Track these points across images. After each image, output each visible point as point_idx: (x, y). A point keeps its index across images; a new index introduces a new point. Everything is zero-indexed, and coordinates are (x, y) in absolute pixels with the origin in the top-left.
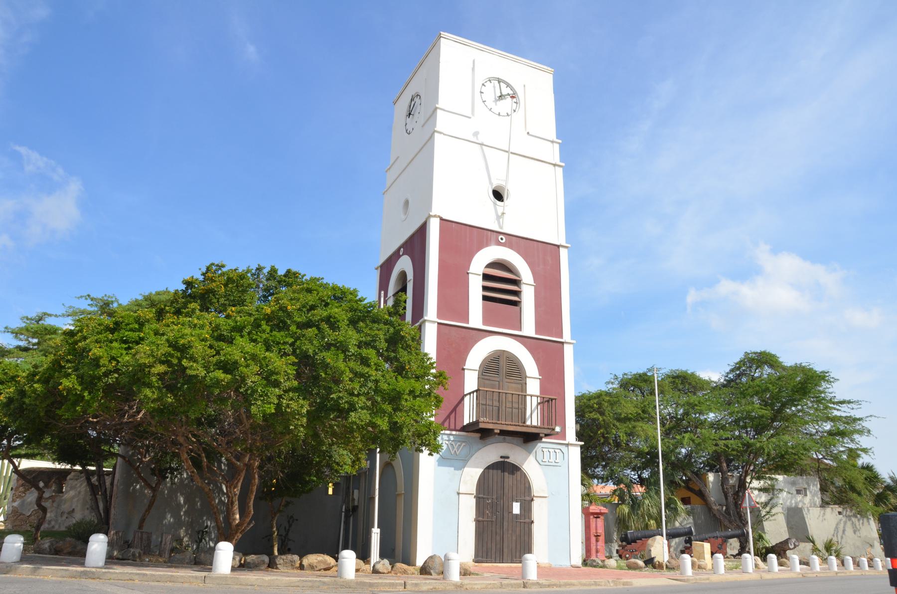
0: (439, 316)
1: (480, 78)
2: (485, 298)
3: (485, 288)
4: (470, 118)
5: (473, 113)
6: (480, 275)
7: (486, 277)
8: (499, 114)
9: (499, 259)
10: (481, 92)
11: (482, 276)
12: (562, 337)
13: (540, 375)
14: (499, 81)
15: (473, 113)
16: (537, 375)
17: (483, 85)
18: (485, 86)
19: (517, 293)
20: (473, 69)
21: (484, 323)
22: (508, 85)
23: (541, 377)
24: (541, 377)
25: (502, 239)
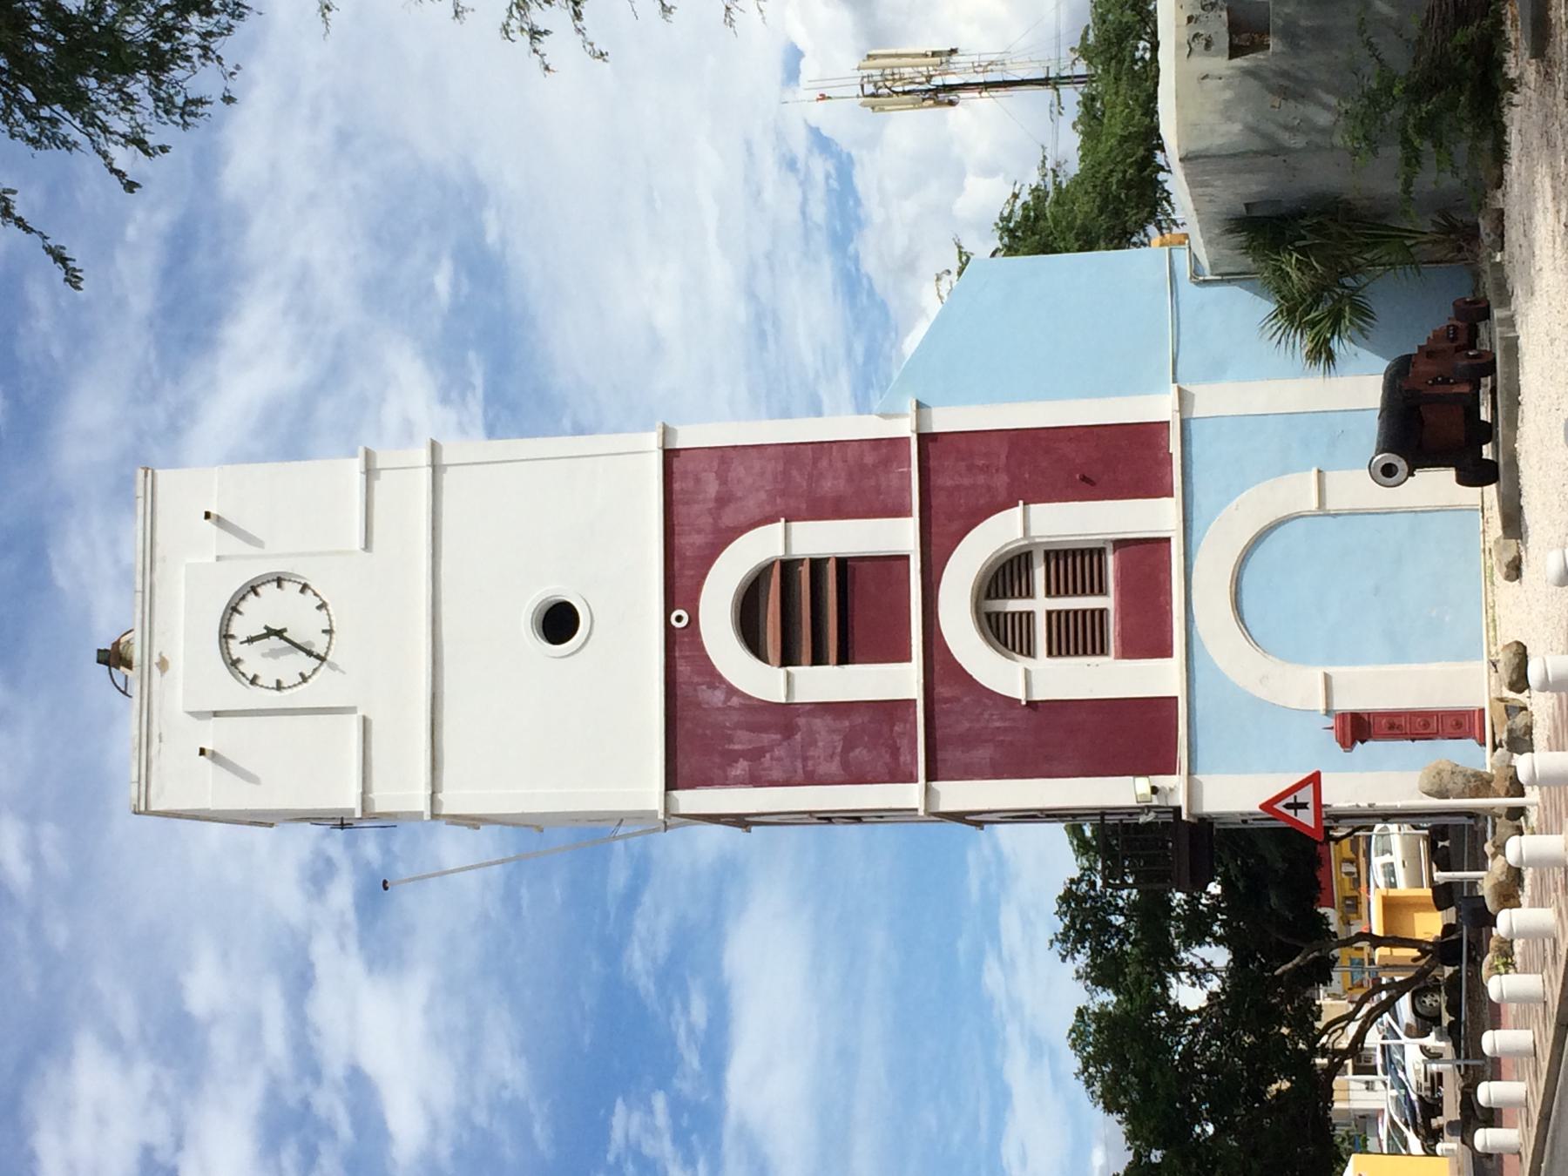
0: (912, 779)
1: (238, 695)
2: (844, 659)
3: (818, 659)
4: (365, 720)
5: (350, 710)
6: (788, 675)
7: (788, 658)
8: (329, 632)
9: (735, 624)
10: (279, 686)
11: (790, 669)
12: (906, 440)
13: (1017, 505)
14: (225, 636)
15: (350, 710)
16: (1017, 511)
17: (253, 681)
18: (255, 677)
19: (817, 565)
20: (216, 714)
21: (905, 657)
22: (233, 609)
23: (1021, 502)
24: (1021, 502)
25: (679, 619)
